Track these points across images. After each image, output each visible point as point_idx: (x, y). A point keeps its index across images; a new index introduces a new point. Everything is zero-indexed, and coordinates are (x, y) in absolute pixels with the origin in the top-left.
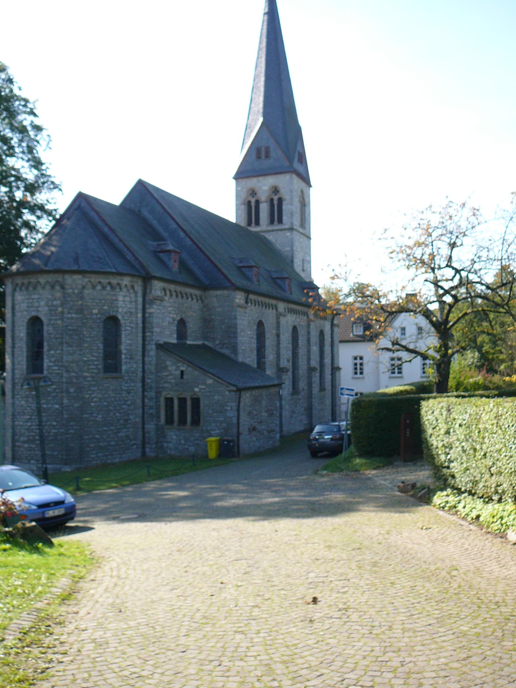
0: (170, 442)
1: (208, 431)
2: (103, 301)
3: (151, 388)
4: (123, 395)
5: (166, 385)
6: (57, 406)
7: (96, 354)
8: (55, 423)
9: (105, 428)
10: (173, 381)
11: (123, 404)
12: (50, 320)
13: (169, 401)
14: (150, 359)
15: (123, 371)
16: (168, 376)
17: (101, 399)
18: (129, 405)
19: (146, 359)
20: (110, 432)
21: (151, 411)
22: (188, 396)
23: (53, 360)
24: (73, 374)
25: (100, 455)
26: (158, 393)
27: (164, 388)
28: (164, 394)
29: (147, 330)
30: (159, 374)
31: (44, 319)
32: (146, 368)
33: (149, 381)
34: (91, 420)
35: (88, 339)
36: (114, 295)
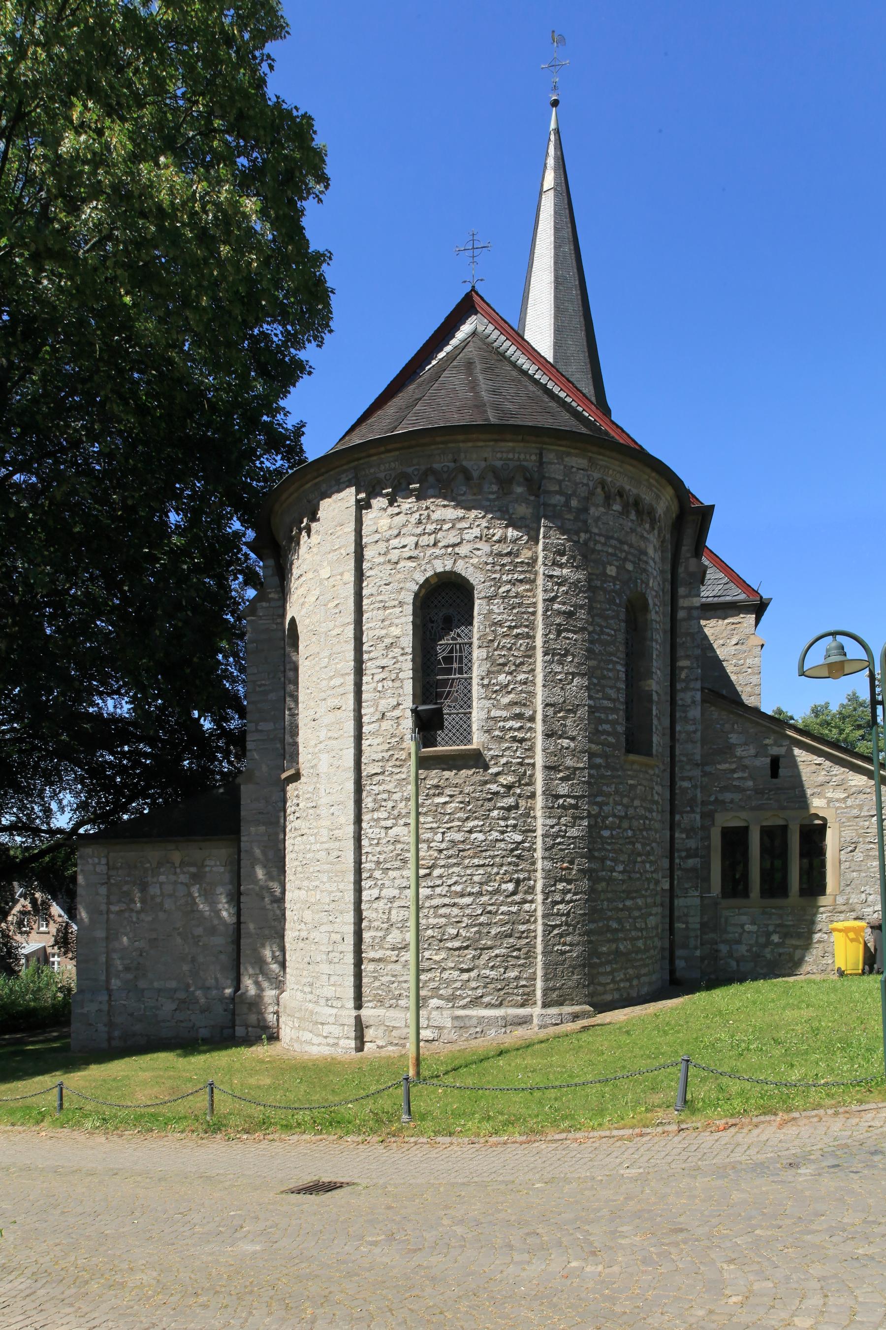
0: (739, 942)
3: (692, 803)
5: (728, 796)
6: (518, 838)
7: (612, 693)
8: (510, 887)
9: (629, 903)
10: (750, 783)
12: (498, 583)
13: (734, 840)
14: (691, 728)
15: (654, 752)
16: (734, 771)
17: (621, 818)
19: (678, 728)
20: (636, 913)
21: (691, 862)
24: (565, 742)
25: (620, 976)
26: (708, 816)
29: (680, 652)
30: (708, 769)
31: (475, 578)
32: (677, 752)
33: (686, 784)
34: (603, 879)
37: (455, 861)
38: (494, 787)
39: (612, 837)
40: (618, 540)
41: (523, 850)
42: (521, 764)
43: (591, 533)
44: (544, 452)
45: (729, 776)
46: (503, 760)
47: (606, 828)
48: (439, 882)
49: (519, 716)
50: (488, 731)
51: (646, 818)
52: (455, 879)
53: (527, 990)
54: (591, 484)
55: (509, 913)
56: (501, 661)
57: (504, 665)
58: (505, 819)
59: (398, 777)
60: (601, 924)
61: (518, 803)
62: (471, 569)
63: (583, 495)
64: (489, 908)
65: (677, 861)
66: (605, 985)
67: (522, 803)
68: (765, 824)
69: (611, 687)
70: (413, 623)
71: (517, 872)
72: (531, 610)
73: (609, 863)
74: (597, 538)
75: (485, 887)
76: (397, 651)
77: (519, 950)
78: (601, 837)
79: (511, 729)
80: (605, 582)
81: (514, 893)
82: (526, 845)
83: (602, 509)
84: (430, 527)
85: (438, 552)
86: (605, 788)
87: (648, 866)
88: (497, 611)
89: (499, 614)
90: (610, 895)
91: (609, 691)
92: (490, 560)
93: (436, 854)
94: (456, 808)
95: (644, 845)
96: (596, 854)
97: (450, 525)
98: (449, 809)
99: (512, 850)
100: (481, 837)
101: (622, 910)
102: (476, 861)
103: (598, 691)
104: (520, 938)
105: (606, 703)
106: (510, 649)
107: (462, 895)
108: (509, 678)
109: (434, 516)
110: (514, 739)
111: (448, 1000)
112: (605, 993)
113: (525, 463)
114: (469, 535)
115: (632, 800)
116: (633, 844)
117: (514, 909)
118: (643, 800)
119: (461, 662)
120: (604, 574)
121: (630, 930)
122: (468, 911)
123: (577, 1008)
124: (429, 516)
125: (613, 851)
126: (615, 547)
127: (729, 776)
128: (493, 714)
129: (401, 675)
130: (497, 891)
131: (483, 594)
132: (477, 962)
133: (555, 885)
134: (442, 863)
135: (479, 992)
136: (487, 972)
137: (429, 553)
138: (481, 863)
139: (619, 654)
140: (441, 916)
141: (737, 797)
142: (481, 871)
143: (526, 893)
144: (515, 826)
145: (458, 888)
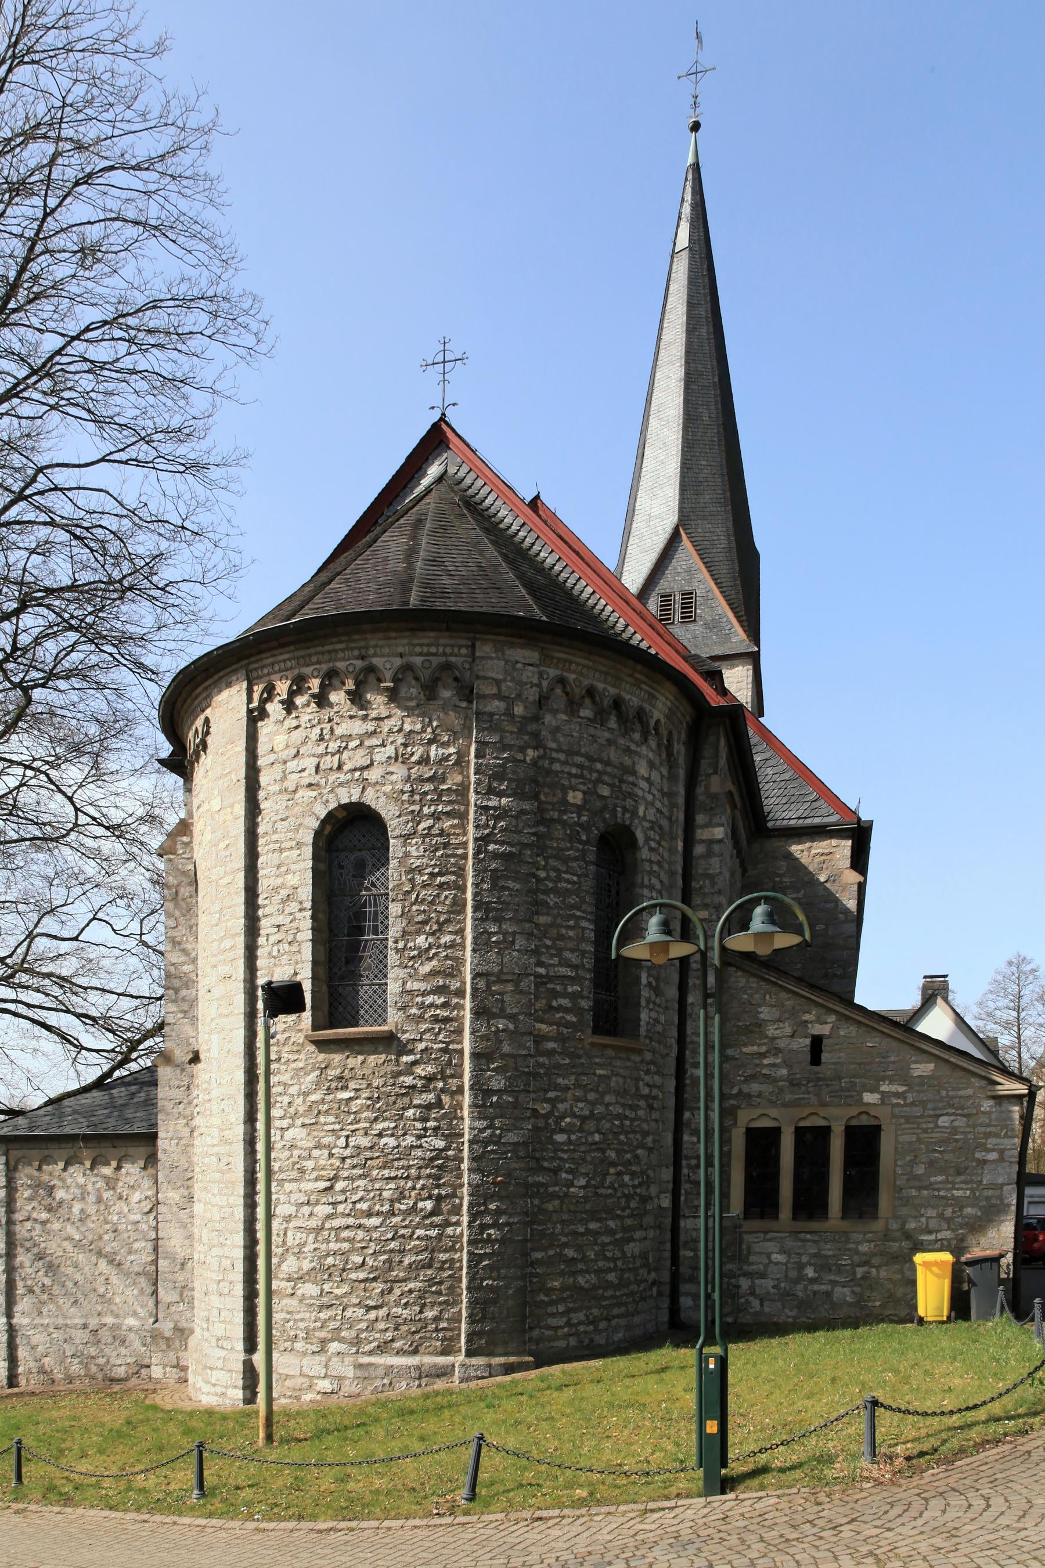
1: (908, 1236)
2: (599, 766)
4: (641, 1113)
5: (755, 1087)
6: (440, 1144)
7: (573, 957)
8: (429, 1205)
9: (593, 1226)
10: (784, 1072)
11: (642, 1146)
13: (762, 1144)
17: (584, 1119)
18: (650, 1150)
20: (606, 1239)
22: (837, 1120)
23: (426, 968)
25: (578, 1317)
27: (749, 1096)
28: (747, 1117)
34: (554, 1196)
35: (552, 899)
36: (628, 751)
37: (361, 1172)
38: (408, 1080)
39: (569, 1142)
40: (587, 756)
41: (447, 1158)
42: (445, 1050)
43: (545, 748)
44: (478, 644)
45: (757, 1061)
46: (421, 1046)
47: (562, 1131)
48: (342, 1198)
49: (439, 990)
50: (403, 1008)
51: (626, 1117)
52: (360, 1194)
53: (449, 1334)
54: (545, 684)
55: (428, 1238)
56: (420, 918)
57: (425, 922)
58: (425, 1120)
59: (294, 1065)
60: (551, 1253)
61: (440, 1100)
62: (383, 799)
63: (531, 698)
64: (402, 1232)
65: (685, 1171)
66: (556, 1328)
67: (446, 1099)
68: (802, 1124)
69: (572, 951)
70: (314, 869)
71: (438, 1186)
72: (460, 852)
73: (564, 1175)
74: (555, 755)
75: (397, 1205)
76: (294, 906)
77: (440, 1283)
78: (553, 1142)
79: (432, 1005)
80: (565, 812)
81: (433, 1213)
82: (451, 1153)
83: (564, 717)
84: (333, 746)
85: (342, 777)
86: (560, 1080)
87: (626, 1178)
88: (415, 854)
89: (418, 858)
90: (565, 1217)
91: (567, 955)
92: (407, 787)
93: (338, 1163)
94: (362, 1105)
95: (619, 1152)
96: (546, 1164)
97: (358, 742)
98: (354, 1106)
99: (432, 1159)
100: (392, 1142)
101: (583, 1234)
102: (386, 1173)
103: (552, 956)
104: (442, 1269)
105: (563, 971)
106: (432, 903)
107: (369, 1214)
108: (431, 940)
109: (339, 731)
110: (436, 1019)
111: (352, 1344)
112: (556, 1338)
113: (453, 659)
114: (381, 755)
115: (602, 1095)
116: (603, 1151)
117: (433, 1233)
118: (617, 1093)
119: (376, 919)
120: (564, 801)
121: (596, 1261)
122: (375, 1235)
123: (512, 1359)
124: (332, 730)
125: (572, 1160)
126: (581, 766)
127: (757, 1061)
128: (409, 986)
129: (299, 937)
130: (413, 1210)
131: (397, 833)
132: (387, 1298)
133: (485, 1204)
134: (345, 1174)
135: (389, 1335)
136: (398, 1310)
137: (331, 779)
138: (393, 1174)
139: (584, 907)
140: (345, 1240)
141: (766, 1088)
142: (392, 1186)
143: (451, 1212)
144: (436, 1129)
145: (364, 1206)
